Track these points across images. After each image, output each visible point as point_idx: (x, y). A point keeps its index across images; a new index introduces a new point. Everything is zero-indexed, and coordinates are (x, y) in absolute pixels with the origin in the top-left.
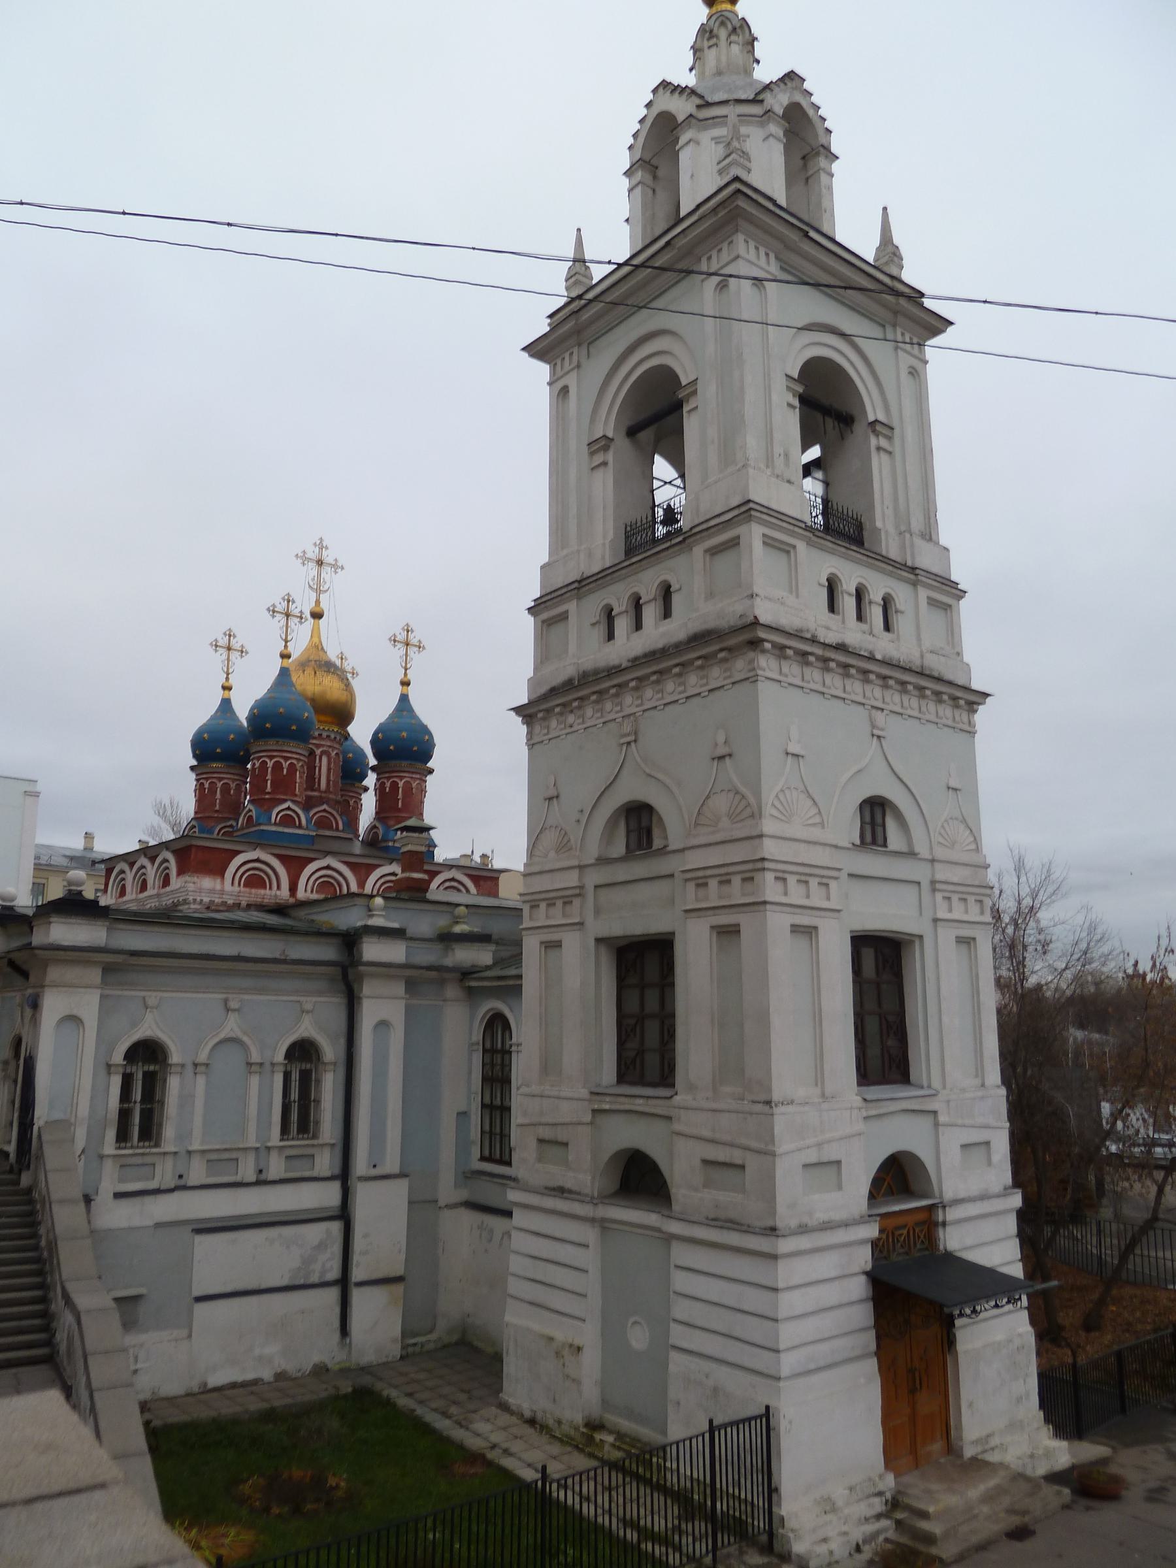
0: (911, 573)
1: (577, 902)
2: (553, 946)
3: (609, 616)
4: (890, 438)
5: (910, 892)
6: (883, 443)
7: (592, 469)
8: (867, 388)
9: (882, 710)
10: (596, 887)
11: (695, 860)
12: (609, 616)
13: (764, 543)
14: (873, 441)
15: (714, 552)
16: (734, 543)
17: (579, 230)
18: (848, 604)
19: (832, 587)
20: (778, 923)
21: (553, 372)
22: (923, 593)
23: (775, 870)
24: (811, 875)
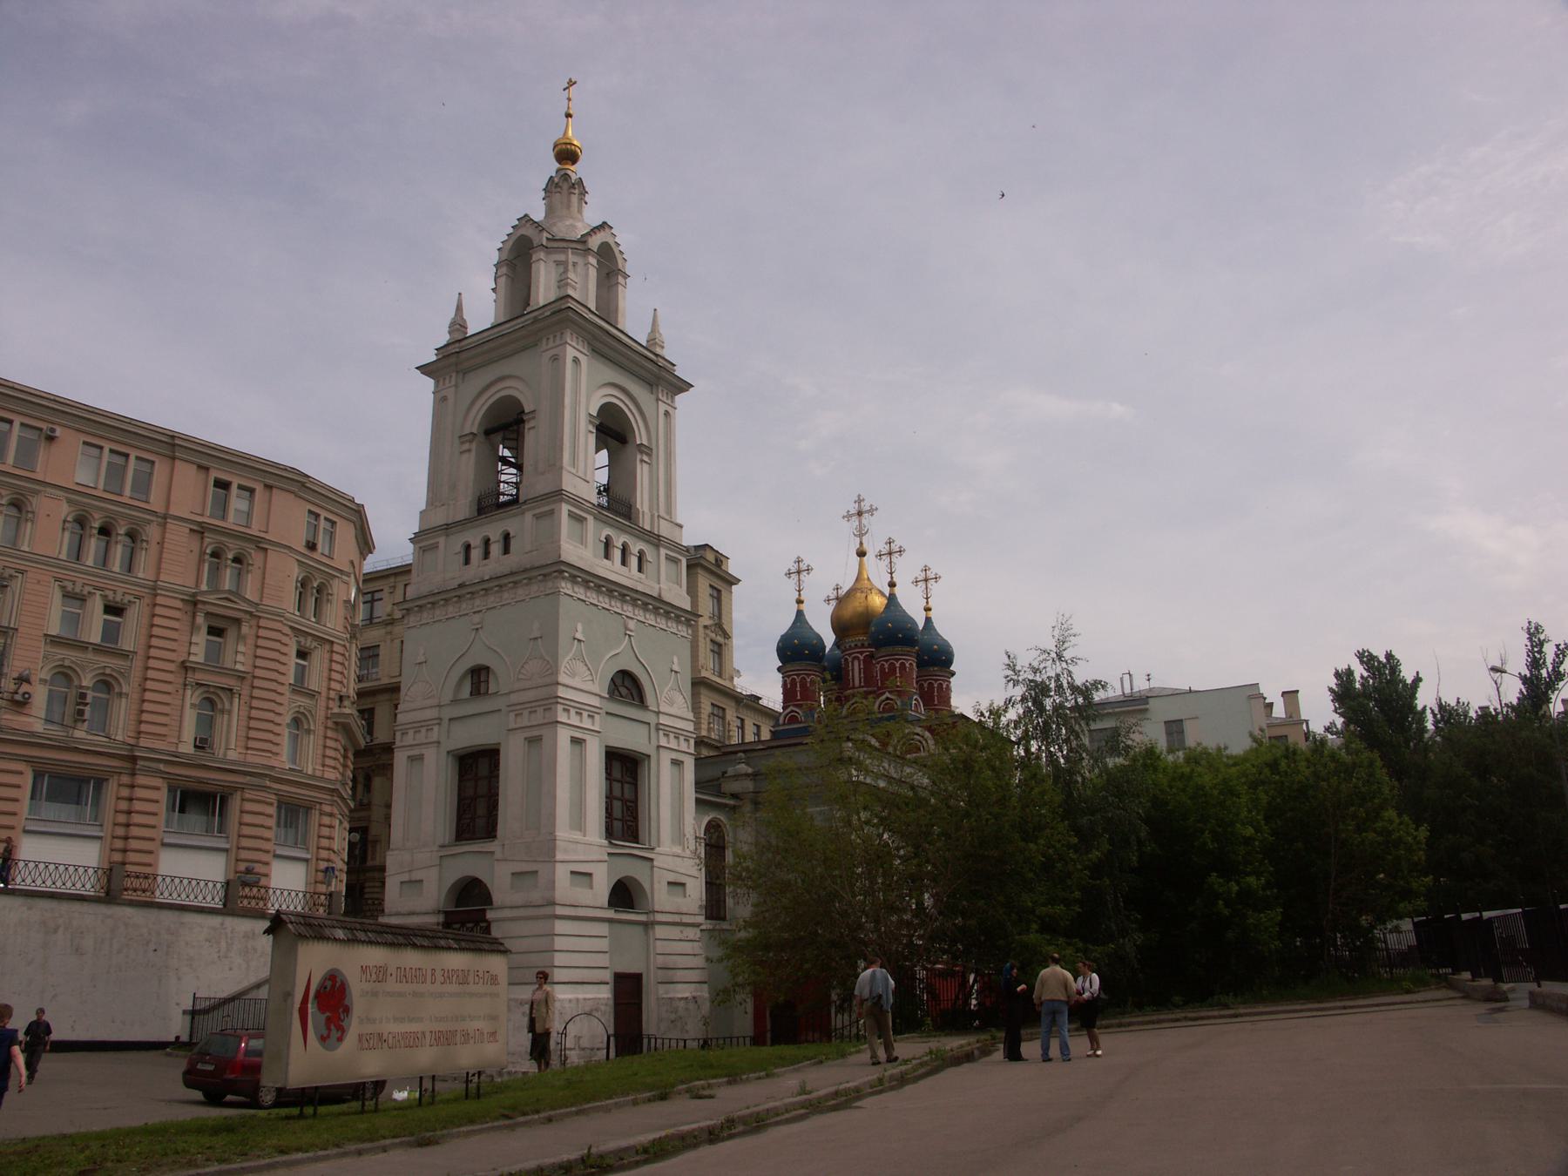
0: (655, 540)
1: (436, 728)
2: (416, 759)
3: (468, 548)
4: (649, 455)
5: (643, 729)
6: (645, 458)
7: (461, 453)
8: (638, 426)
9: (632, 618)
10: (450, 720)
11: (514, 698)
12: (468, 548)
13: (569, 515)
14: (639, 457)
15: (538, 517)
16: (552, 512)
17: (460, 294)
18: (617, 554)
19: (608, 544)
20: (564, 736)
21: (437, 385)
22: (663, 551)
23: (563, 704)
24: (584, 710)
